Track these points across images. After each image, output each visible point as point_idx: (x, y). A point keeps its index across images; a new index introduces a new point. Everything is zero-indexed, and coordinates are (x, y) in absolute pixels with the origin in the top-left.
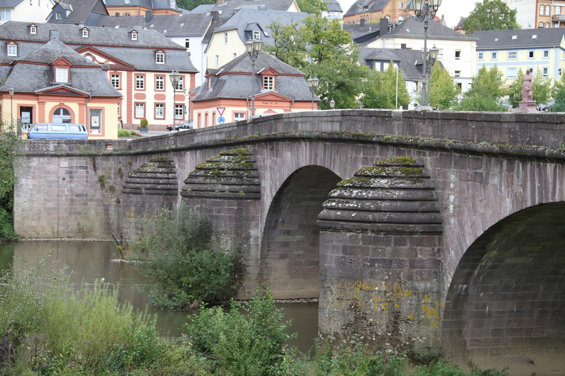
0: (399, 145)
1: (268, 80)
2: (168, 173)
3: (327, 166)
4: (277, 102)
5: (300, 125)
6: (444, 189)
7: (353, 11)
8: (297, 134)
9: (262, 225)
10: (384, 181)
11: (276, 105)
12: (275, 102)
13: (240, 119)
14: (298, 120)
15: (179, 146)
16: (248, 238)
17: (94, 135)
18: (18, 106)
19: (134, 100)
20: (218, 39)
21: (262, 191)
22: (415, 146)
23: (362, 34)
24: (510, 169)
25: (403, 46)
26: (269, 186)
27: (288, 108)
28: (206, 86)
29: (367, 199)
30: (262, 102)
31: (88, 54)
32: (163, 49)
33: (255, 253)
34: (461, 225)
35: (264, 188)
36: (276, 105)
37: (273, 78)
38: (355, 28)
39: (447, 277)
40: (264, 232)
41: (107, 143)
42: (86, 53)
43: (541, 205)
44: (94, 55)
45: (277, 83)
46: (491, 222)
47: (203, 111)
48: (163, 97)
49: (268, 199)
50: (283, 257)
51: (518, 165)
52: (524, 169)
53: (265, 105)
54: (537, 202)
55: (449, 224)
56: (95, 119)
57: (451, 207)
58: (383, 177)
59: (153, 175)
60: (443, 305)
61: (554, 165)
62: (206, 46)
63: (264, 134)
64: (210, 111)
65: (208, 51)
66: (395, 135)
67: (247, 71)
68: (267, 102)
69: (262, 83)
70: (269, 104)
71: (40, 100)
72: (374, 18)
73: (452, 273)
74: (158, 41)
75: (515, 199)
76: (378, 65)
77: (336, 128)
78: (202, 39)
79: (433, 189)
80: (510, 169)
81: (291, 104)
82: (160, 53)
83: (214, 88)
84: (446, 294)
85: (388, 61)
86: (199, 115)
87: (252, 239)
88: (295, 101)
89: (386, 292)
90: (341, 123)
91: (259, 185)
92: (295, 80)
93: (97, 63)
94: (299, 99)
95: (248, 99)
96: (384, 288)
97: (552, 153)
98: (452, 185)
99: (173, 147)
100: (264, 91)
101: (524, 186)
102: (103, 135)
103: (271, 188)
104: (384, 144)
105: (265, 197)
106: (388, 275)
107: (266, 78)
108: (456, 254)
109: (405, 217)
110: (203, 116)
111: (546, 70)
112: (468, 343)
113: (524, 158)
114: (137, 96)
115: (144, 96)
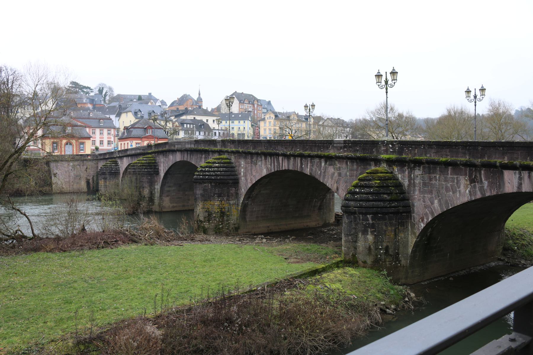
0: (220, 152)
1: (149, 130)
2: (116, 166)
3: (189, 160)
5: (176, 146)
6: (239, 167)
7: (172, 104)
8: (175, 149)
9: (160, 184)
10: (217, 165)
13: (138, 145)
14: (175, 144)
15: (121, 155)
16: (155, 189)
17: (82, 153)
20: (123, 116)
21: (160, 171)
22: (227, 152)
23: (178, 114)
24: (266, 159)
25: (194, 118)
26: (162, 169)
28: (124, 133)
29: (212, 171)
32: (103, 119)
33: (157, 195)
34: (246, 180)
35: (161, 170)
38: (175, 111)
39: (241, 199)
40: (161, 187)
41: (88, 155)
43: (277, 171)
45: (152, 131)
46: (258, 178)
47: (123, 143)
48: (103, 138)
49: (162, 174)
50: (168, 196)
51: (269, 158)
52: (271, 159)
54: (276, 170)
55: (241, 179)
56: (82, 146)
57: (242, 173)
58: (217, 163)
59: (110, 167)
60: (239, 208)
61: (282, 157)
62: (118, 118)
63: (160, 149)
64: (126, 142)
65: (120, 120)
66: (219, 148)
67: (141, 127)
70: (149, 139)
72: (182, 108)
73: (243, 197)
74: (100, 116)
75: (267, 169)
76: (185, 125)
77: (193, 146)
78: (115, 115)
79: (235, 167)
80: (266, 159)
82: (102, 121)
83: (127, 134)
84: (240, 205)
85: (189, 124)
86: (121, 144)
87: (156, 190)
88: (160, 138)
89: (219, 205)
90: (194, 144)
91: (158, 169)
92: (159, 130)
94: (161, 137)
96: (218, 204)
97: (282, 153)
98: (242, 166)
99: (118, 156)
100: (147, 135)
101: (271, 165)
102: (85, 152)
103: (163, 169)
104: (214, 152)
105: (161, 173)
106: (220, 199)
108: (244, 190)
109: (225, 177)
110: (126, 144)
111: (244, 128)
112: (248, 222)
113: (271, 155)
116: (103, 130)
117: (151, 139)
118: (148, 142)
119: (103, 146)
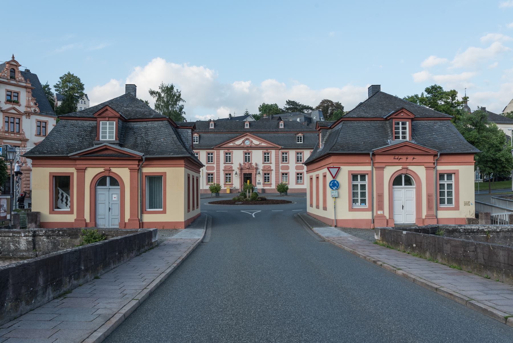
1: (401, 126)
4: (415, 157)
11: (414, 161)
12: (412, 157)
18: (50, 176)
19: (281, 171)
27: (432, 165)
30: (393, 157)
31: (247, 139)
36: (414, 161)
37: (408, 123)
42: (246, 138)
44: (251, 139)
53: (397, 161)
68: (400, 157)
69: (392, 130)
70: (404, 159)
71: (78, 166)
81: (436, 158)
93: (254, 145)
95: (371, 153)
107: (398, 124)
114: (283, 168)
115: (287, 168)
116: (303, 152)
117: (410, 159)
118: (400, 168)
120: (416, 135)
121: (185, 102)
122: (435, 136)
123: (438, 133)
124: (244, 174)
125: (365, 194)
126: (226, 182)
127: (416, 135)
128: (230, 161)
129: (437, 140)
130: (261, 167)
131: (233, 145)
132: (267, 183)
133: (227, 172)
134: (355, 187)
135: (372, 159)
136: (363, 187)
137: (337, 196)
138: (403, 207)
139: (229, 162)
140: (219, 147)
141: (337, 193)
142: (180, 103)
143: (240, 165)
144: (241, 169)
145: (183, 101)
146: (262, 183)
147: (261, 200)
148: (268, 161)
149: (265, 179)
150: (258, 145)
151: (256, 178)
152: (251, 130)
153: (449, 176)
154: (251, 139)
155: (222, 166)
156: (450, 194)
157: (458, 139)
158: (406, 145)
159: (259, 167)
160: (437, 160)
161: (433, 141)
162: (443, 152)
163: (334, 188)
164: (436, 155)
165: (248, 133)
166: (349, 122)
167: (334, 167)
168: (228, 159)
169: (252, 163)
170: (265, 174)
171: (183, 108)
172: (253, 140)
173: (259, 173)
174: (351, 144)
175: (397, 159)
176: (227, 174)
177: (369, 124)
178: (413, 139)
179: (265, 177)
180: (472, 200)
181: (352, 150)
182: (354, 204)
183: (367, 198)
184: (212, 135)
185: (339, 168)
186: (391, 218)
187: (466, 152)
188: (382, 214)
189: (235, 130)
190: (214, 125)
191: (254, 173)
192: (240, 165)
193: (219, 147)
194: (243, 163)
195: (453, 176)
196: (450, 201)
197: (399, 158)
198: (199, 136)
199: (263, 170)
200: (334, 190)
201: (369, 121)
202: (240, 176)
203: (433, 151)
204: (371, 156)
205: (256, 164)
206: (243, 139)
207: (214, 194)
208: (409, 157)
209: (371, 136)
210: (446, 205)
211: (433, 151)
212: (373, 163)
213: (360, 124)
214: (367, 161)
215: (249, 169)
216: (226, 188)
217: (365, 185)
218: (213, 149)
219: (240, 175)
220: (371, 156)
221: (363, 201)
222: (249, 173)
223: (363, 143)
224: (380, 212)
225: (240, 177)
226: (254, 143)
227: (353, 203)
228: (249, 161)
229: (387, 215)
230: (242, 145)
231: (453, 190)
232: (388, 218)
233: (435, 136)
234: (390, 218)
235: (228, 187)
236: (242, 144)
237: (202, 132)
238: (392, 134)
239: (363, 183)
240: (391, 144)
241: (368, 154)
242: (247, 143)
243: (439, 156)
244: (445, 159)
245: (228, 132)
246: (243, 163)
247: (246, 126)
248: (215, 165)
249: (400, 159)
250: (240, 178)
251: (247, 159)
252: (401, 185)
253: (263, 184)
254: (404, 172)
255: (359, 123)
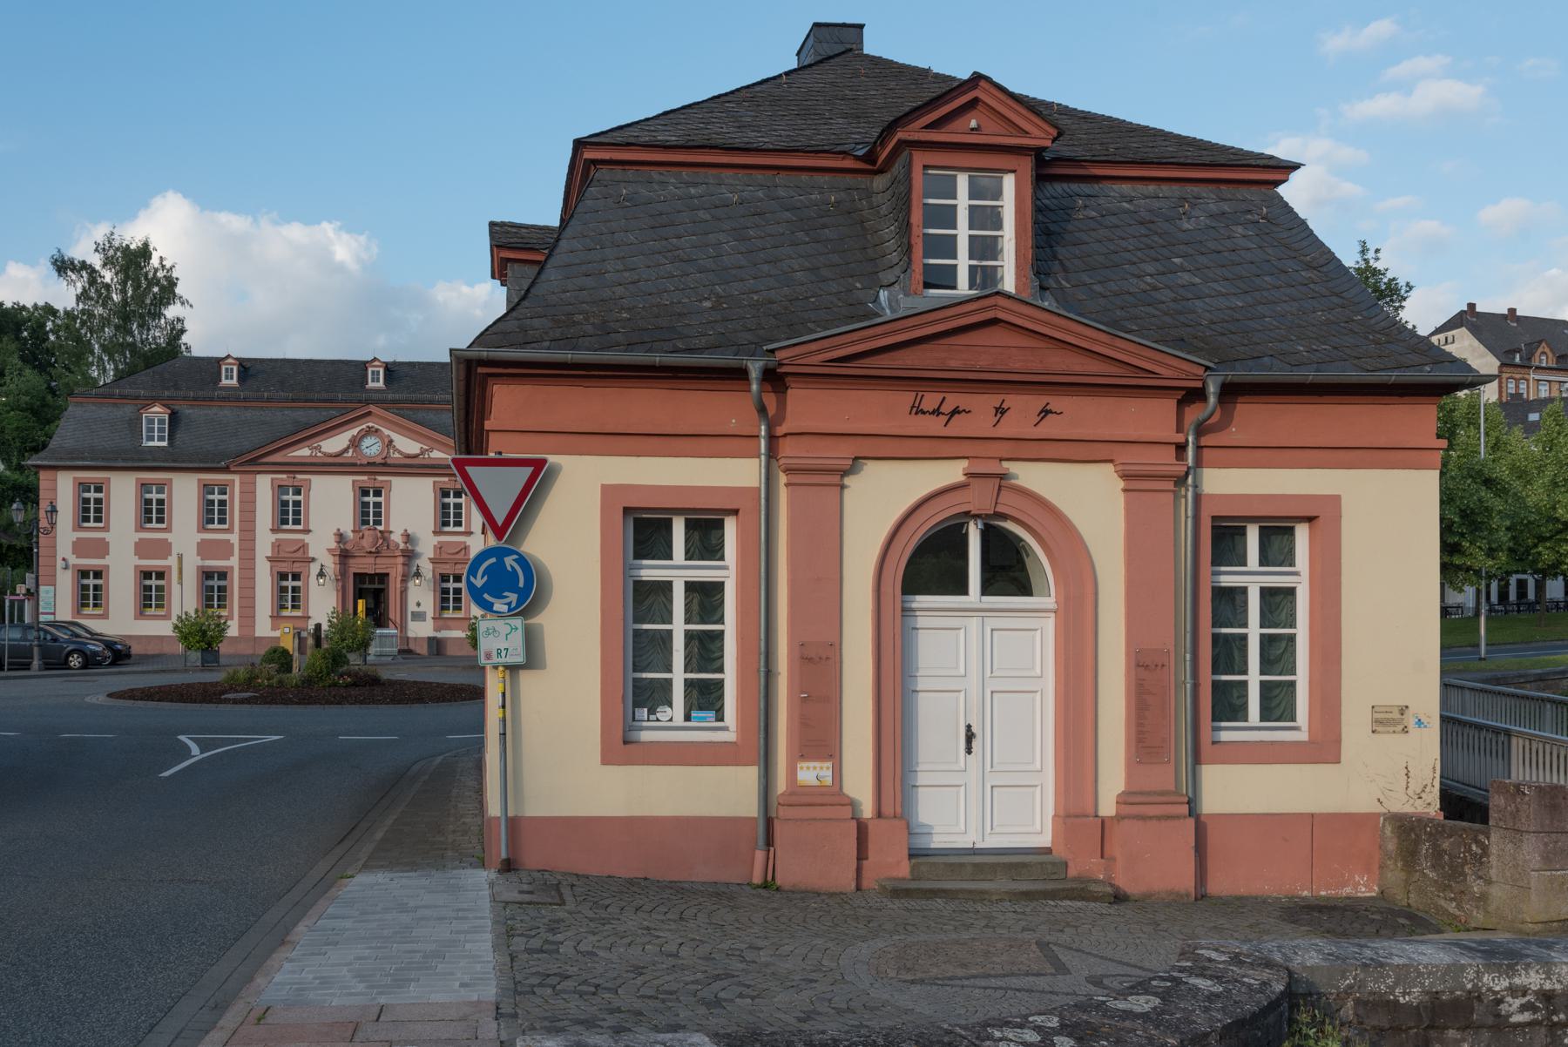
4: (1056, 403)
11: (1049, 428)
12: (1036, 402)
30: (906, 398)
31: (369, 432)
36: (1049, 428)
37: (1009, 182)
42: (364, 426)
44: (387, 432)
53: (934, 425)
68: (953, 400)
69: (905, 228)
70: (979, 412)
81: (1194, 413)
93: (397, 455)
95: (755, 369)
117: (1023, 410)
118: (952, 473)
119: (105, 616)
120: (1065, 270)
121: (191, 306)
122: (1185, 278)
123: (1203, 260)
124: (354, 574)
125: (721, 649)
126: (282, 607)
127: (1065, 270)
128: (297, 522)
129: (1198, 303)
130: (427, 546)
131: (311, 456)
132: (450, 614)
133: (285, 568)
134: (650, 598)
135: (762, 410)
136: (706, 598)
137: (520, 659)
138: (970, 737)
139: (294, 524)
140: (252, 461)
141: (517, 640)
142: (171, 312)
143: (340, 537)
144: (344, 556)
145: (183, 303)
146: (430, 614)
147: (354, 685)
148: (458, 524)
149: (445, 600)
150: (416, 456)
151: (404, 592)
152: (390, 396)
153: (1277, 535)
154: (387, 432)
155: (265, 541)
156: (1277, 653)
157: (1335, 300)
158: (994, 322)
159: (419, 549)
160: (1201, 430)
161: (1172, 305)
162: (1240, 374)
163: (499, 606)
164: (1197, 395)
165: (372, 408)
166: (631, 173)
167: (506, 455)
168: (289, 513)
169: (391, 532)
170: (445, 578)
171: (183, 331)
172: (394, 436)
173: (418, 575)
174: (629, 310)
175: (937, 412)
176: (283, 576)
177: (760, 194)
178: (1043, 288)
179: (445, 591)
180: (1425, 697)
181: (630, 346)
182: (643, 713)
183: (730, 677)
184: (226, 413)
185: (538, 464)
186: (888, 809)
187: (1393, 376)
188: (829, 781)
189: (324, 395)
190: (239, 372)
191: (396, 571)
192: (340, 537)
193: (253, 461)
194: (353, 531)
195: (1302, 534)
196: (1277, 703)
197: (946, 408)
198: (170, 416)
199: (433, 561)
200: (500, 615)
201: (759, 176)
202: (340, 584)
203: (1174, 367)
204: (754, 387)
205: (408, 537)
206: (355, 431)
207: (195, 656)
208: (1015, 401)
209: (766, 268)
210: (1252, 728)
211: (1174, 367)
212: (772, 438)
213: (700, 190)
214: (733, 425)
215: (377, 554)
216: (277, 634)
217: (718, 587)
218: (226, 470)
219: (337, 580)
220: (754, 387)
221: (705, 696)
222: (377, 571)
223: (707, 304)
224: (812, 773)
225: (340, 588)
226: (397, 447)
227: (637, 704)
228: (379, 523)
229: (860, 786)
230: (350, 454)
231: (1302, 632)
232: (867, 811)
233: (1185, 278)
234: (879, 814)
235: (287, 630)
236: (351, 451)
237: (185, 399)
238: (908, 250)
239: (704, 572)
240: (893, 310)
241: (740, 374)
242: (371, 447)
243: (1212, 400)
244: (1253, 420)
245: (293, 401)
246: (353, 531)
247: (373, 381)
248: (234, 538)
249: (956, 411)
250: (337, 590)
251: (369, 512)
252: (963, 590)
253: (433, 618)
254: (980, 499)
255: (695, 185)
